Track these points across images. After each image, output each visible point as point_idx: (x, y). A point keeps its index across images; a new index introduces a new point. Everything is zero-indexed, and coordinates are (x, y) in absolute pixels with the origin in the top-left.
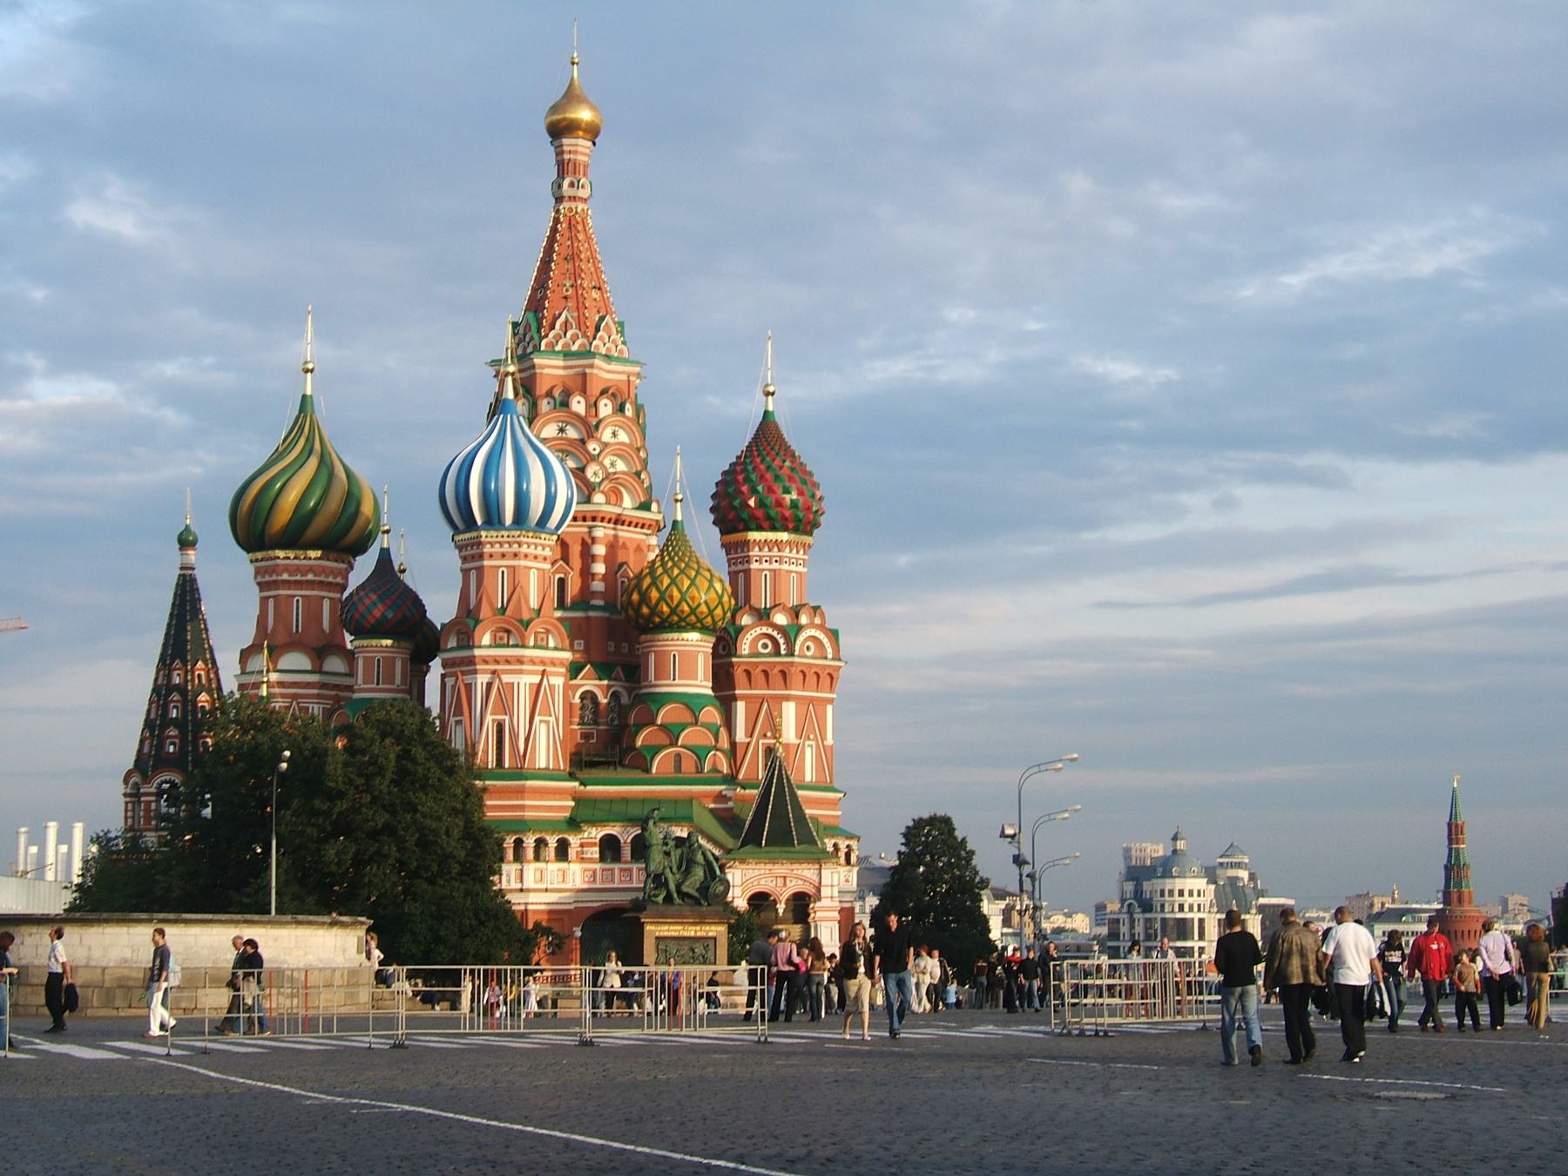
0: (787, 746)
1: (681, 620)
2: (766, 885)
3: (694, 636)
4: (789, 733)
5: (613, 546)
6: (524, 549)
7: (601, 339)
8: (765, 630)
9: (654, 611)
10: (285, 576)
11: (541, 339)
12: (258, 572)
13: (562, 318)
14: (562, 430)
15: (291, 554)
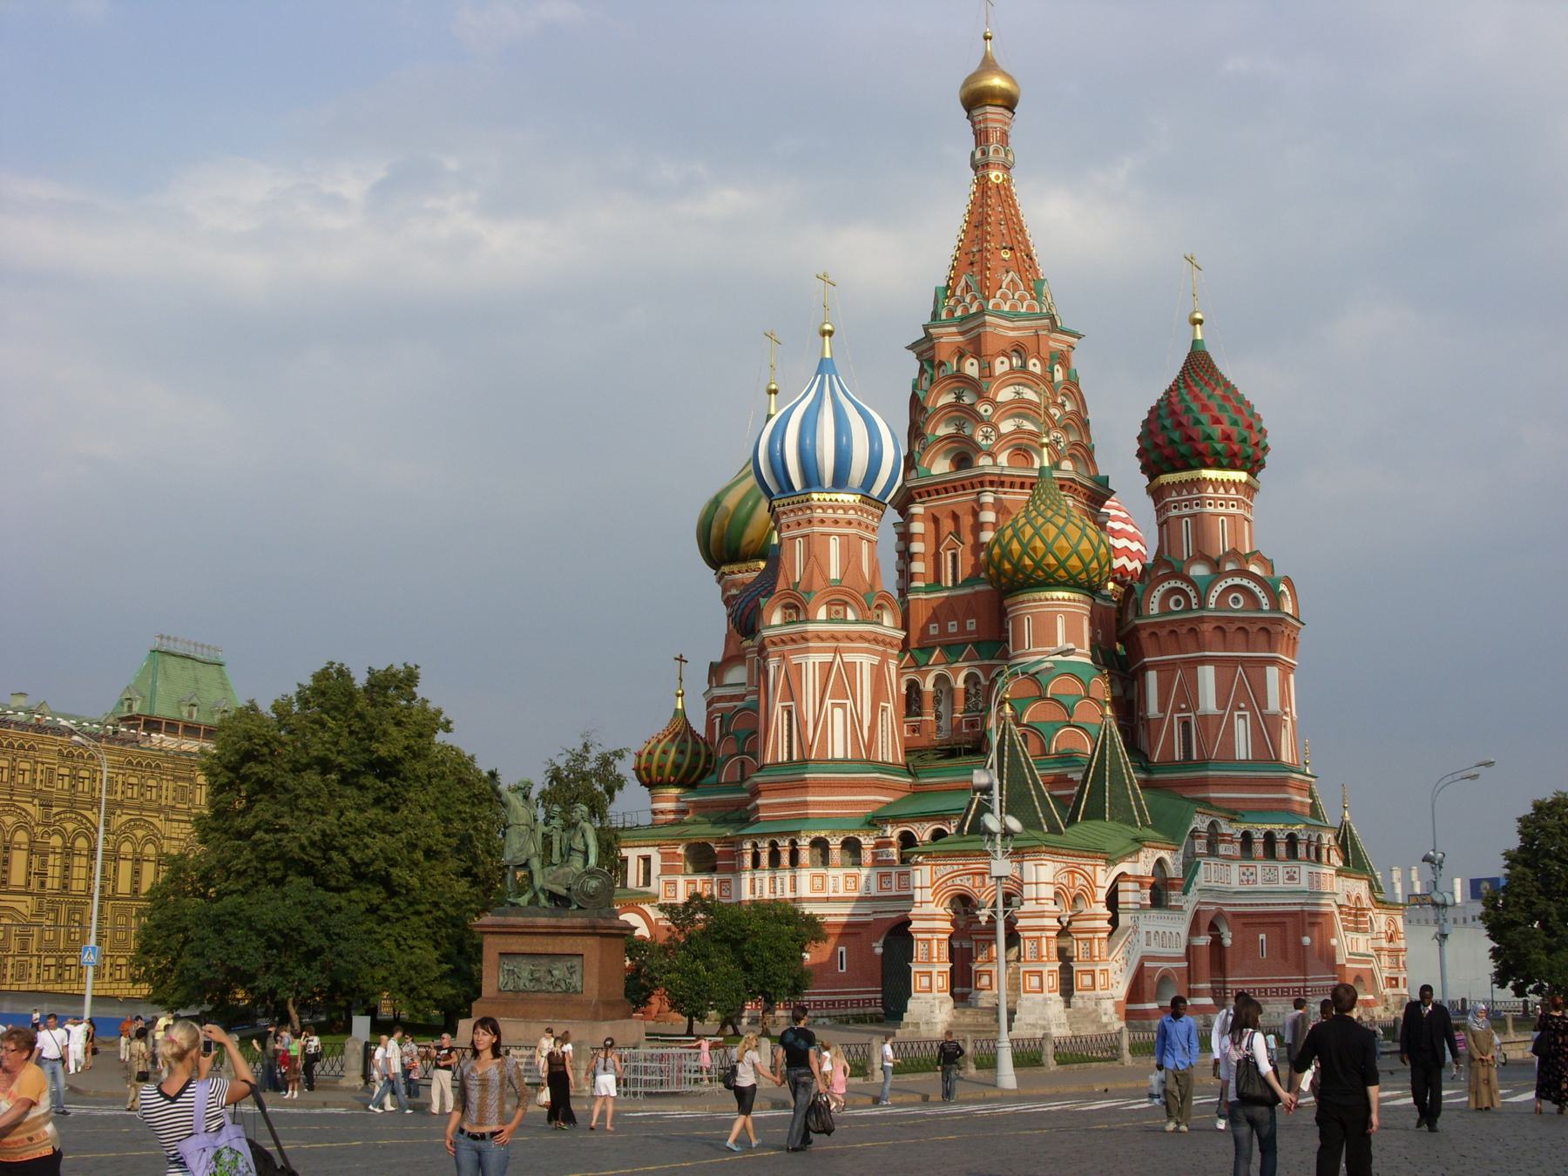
0: (1204, 719)
4: (1208, 701)
6: (819, 513)
8: (1173, 584)
9: (1000, 572)
12: (723, 593)
14: (959, 397)
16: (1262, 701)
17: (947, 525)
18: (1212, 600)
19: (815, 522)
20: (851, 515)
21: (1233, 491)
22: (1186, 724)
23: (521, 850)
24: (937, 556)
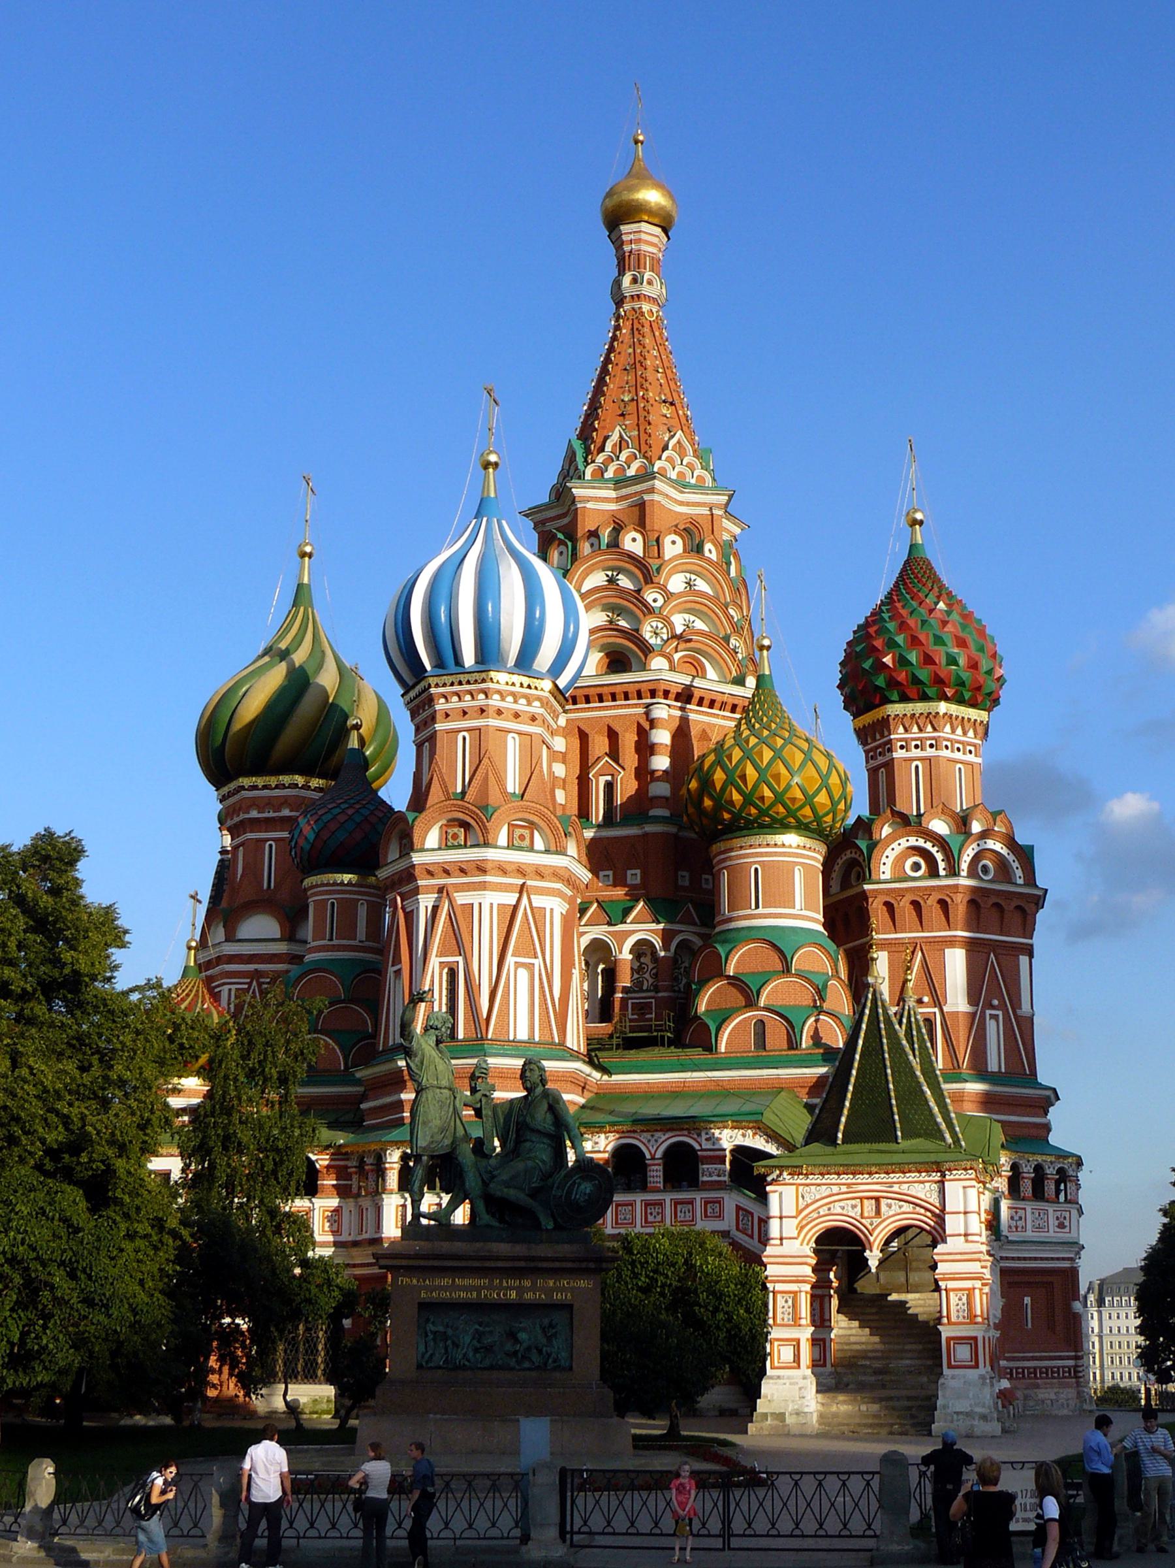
1: (762, 813)
3: (792, 839)
5: (682, 733)
7: (670, 460)
8: (913, 841)
9: (722, 803)
10: (254, 814)
11: (587, 463)
13: (615, 437)
15: (260, 781)
16: (1016, 1003)
17: (599, 745)
18: (964, 866)
19: (491, 711)
20: (536, 708)
21: (971, 733)
23: (443, 1130)
24: (583, 782)
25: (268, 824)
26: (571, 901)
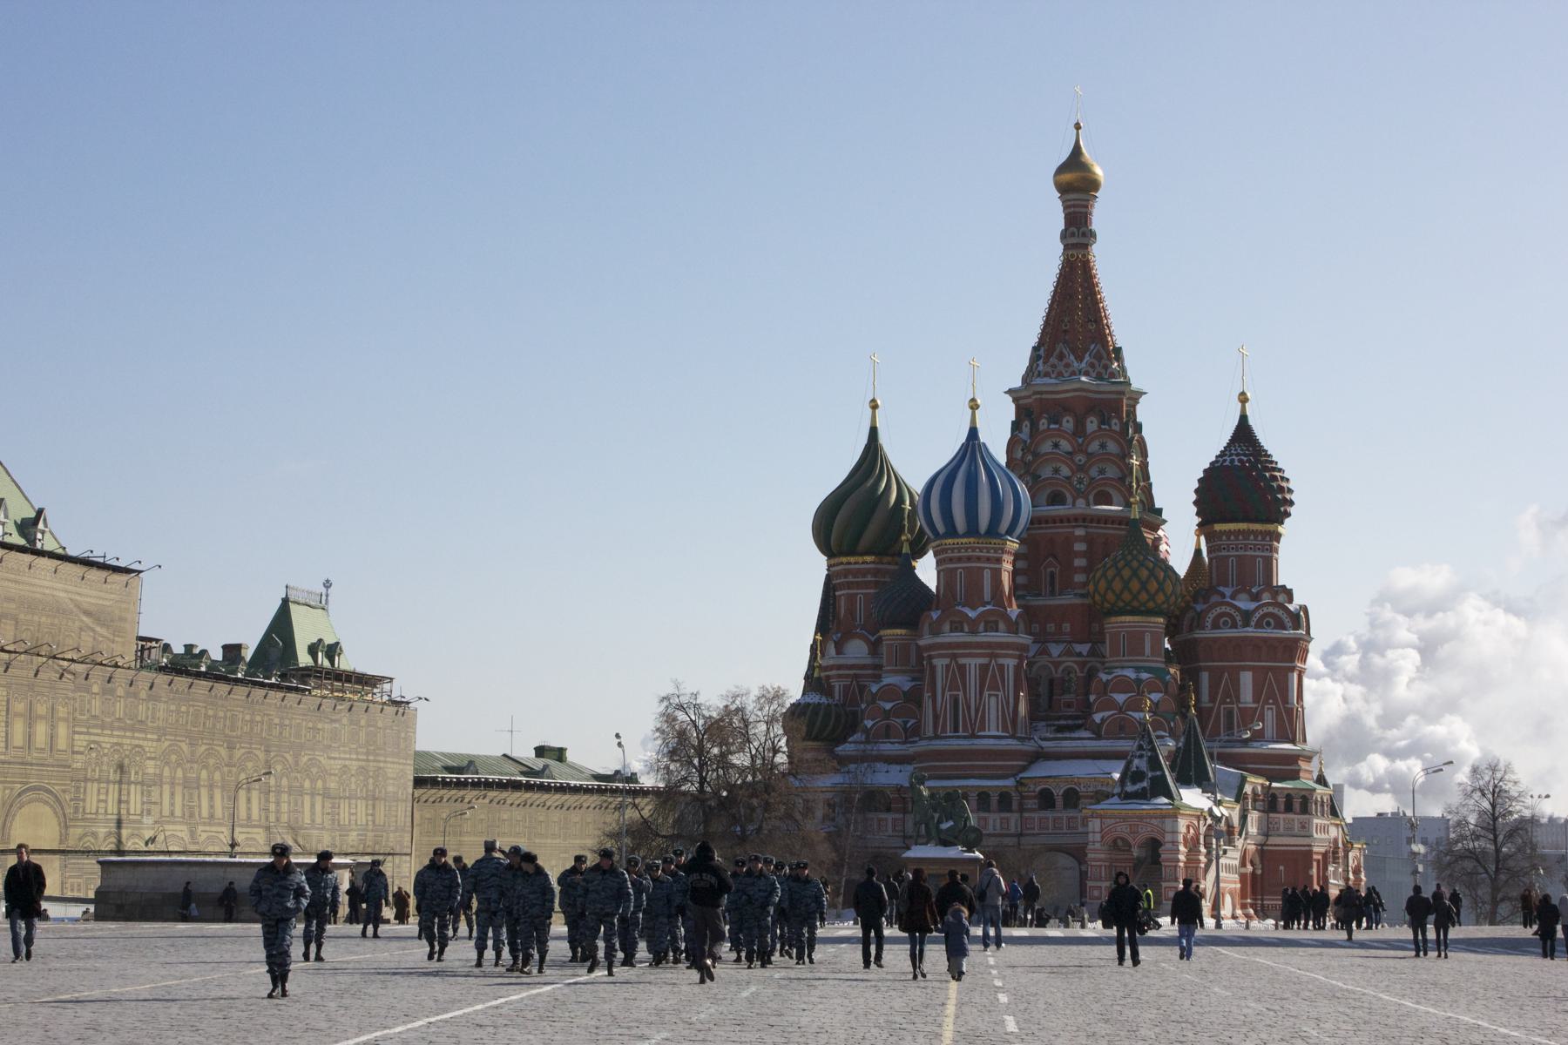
2: (1122, 830)
10: (850, 579)
22: (1230, 713)
25: (859, 585)
26: (1021, 658)
